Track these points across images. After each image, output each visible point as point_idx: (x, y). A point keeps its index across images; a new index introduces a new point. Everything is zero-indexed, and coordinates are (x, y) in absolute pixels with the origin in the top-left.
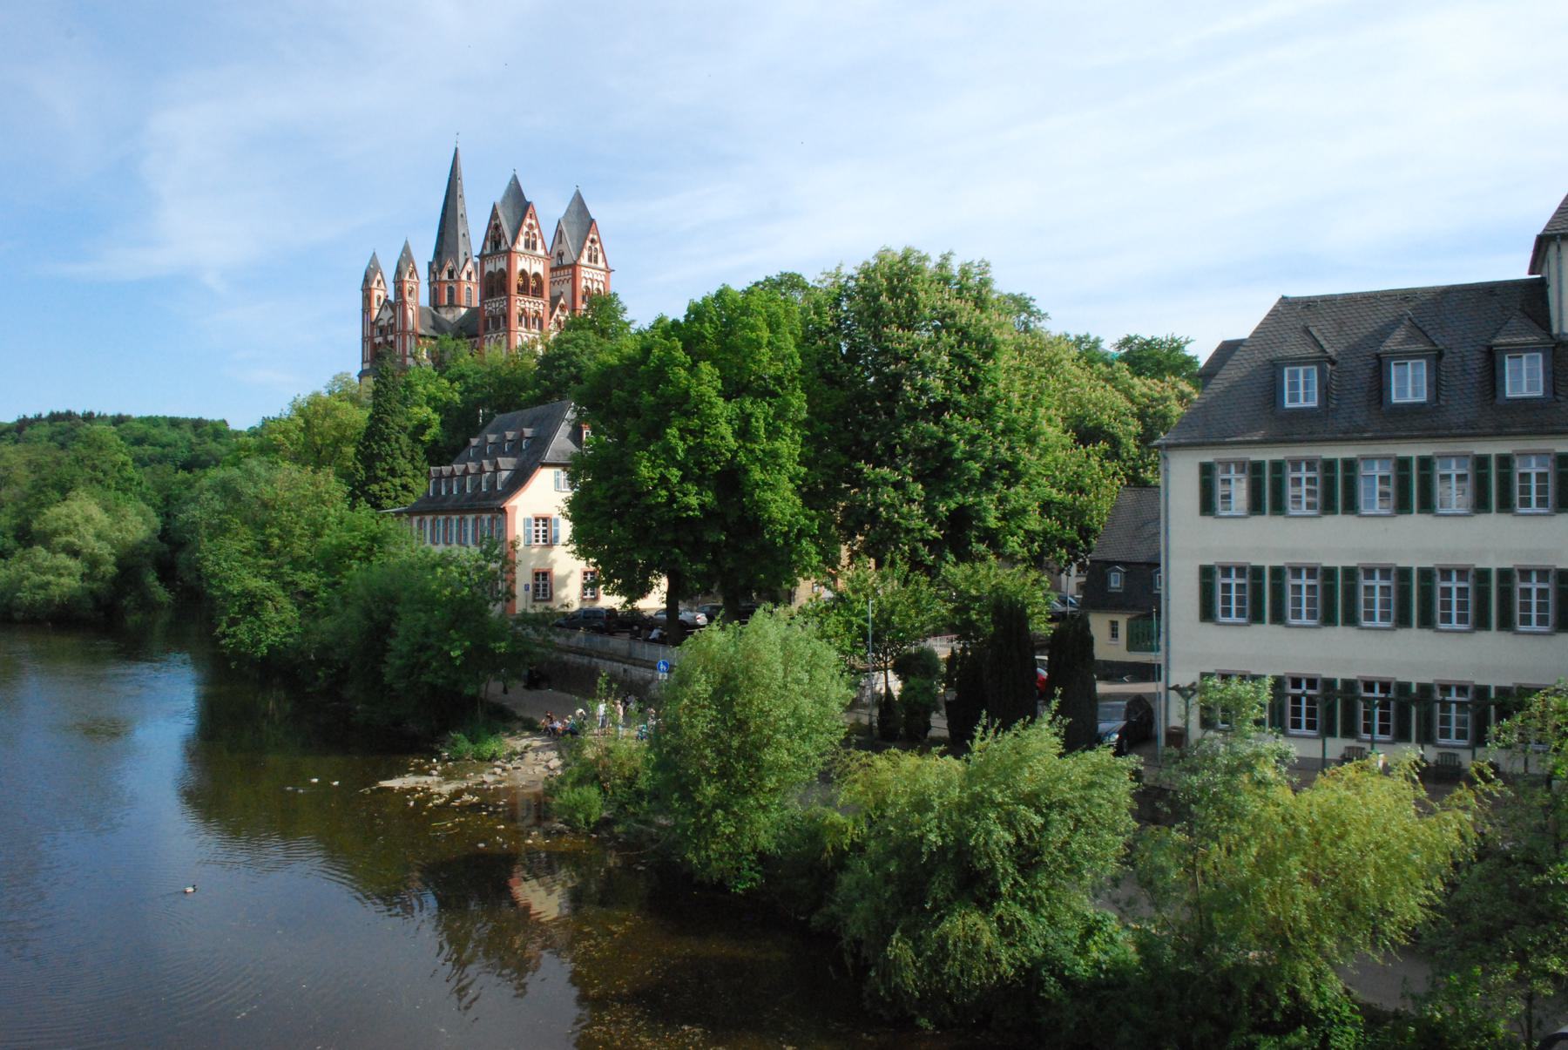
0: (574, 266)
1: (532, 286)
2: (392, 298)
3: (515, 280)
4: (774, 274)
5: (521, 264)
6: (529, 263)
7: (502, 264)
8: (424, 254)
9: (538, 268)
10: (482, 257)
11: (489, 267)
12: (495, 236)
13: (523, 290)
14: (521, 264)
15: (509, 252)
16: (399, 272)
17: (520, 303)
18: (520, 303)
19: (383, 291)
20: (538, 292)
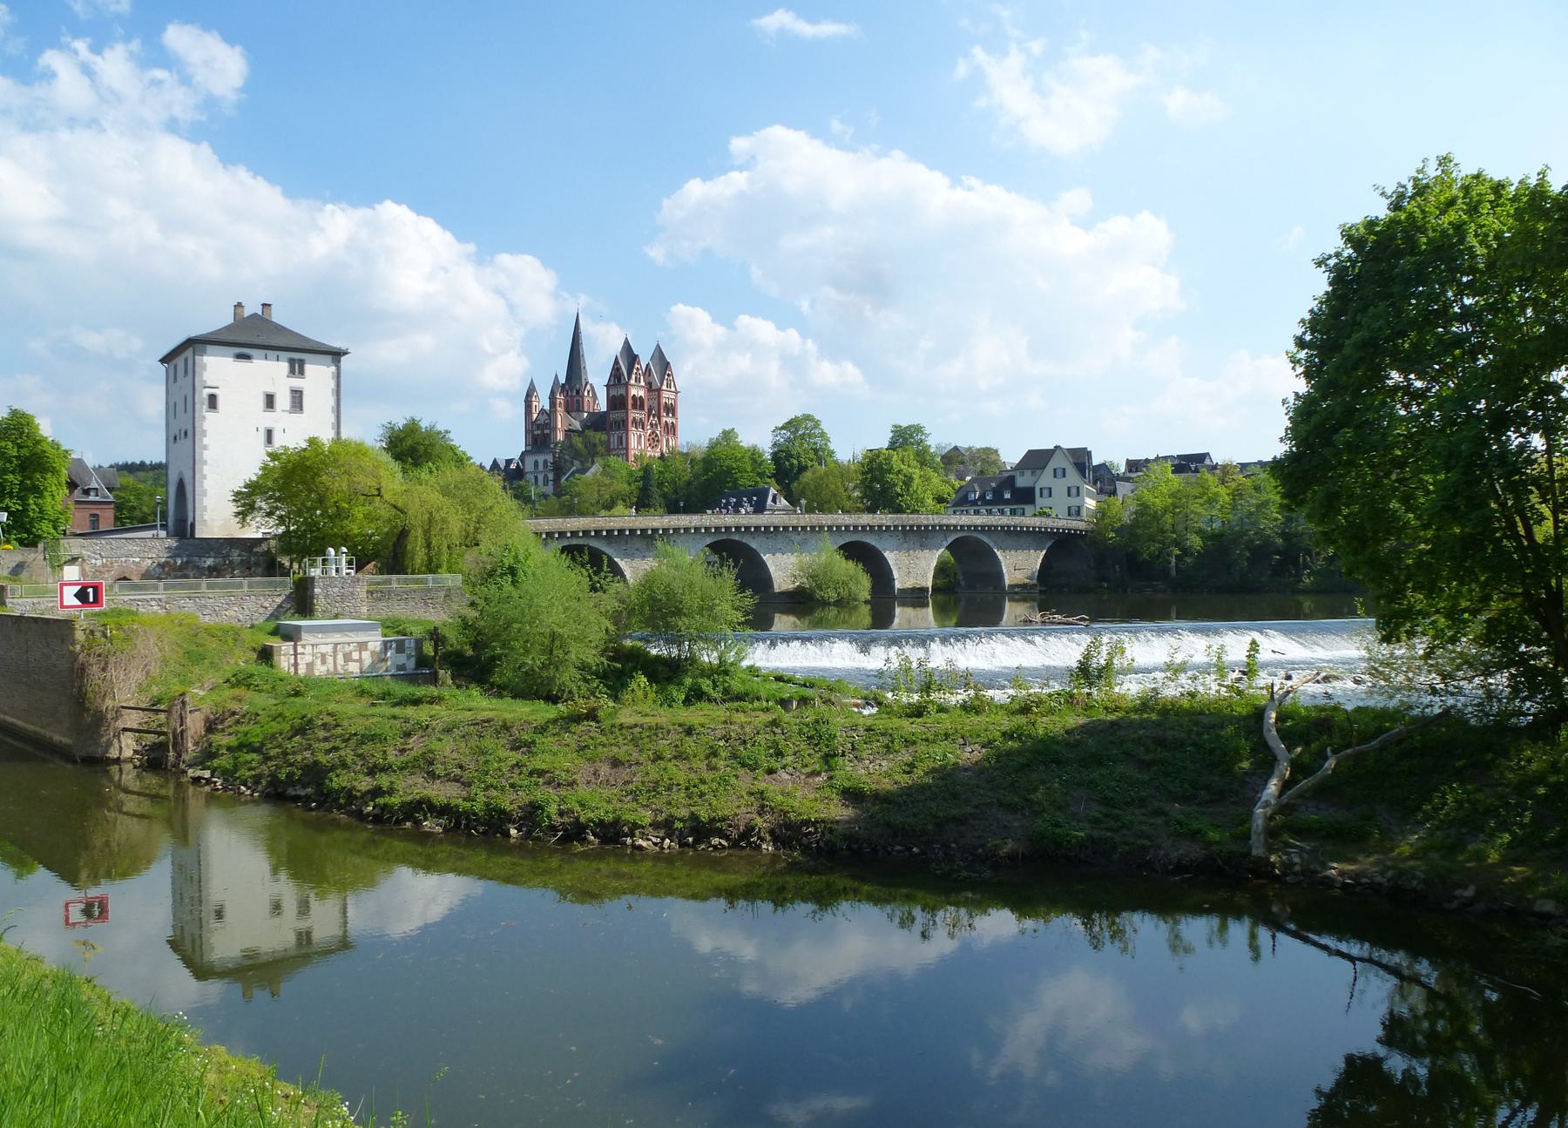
0: (659, 390)
1: (638, 403)
2: (547, 407)
3: (630, 402)
4: (799, 414)
5: (633, 392)
6: (637, 391)
7: (622, 391)
8: (562, 380)
9: (641, 393)
10: (607, 386)
11: (613, 392)
12: (616, 373)
13: (634, 407)
14: (633, 392)
15: (627, 385)
16: (553, 393)
17: (634, 414)
18: (634, 414)
19: (542, 401)
20: (642, 407)
